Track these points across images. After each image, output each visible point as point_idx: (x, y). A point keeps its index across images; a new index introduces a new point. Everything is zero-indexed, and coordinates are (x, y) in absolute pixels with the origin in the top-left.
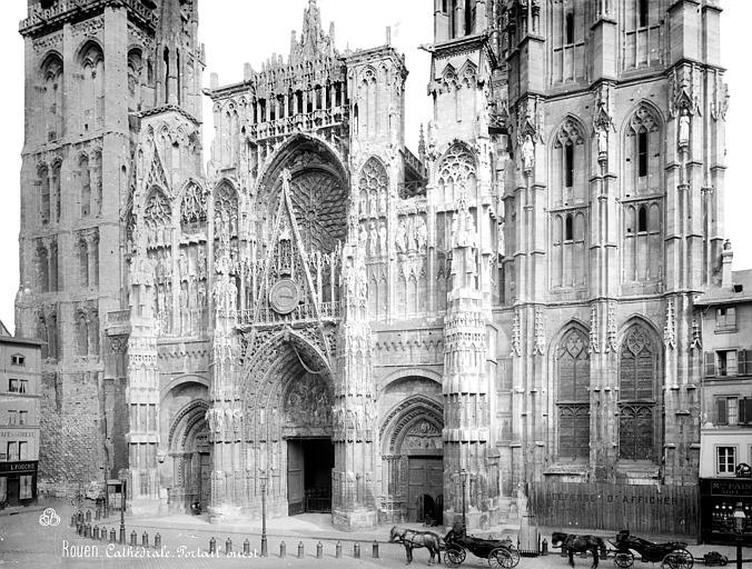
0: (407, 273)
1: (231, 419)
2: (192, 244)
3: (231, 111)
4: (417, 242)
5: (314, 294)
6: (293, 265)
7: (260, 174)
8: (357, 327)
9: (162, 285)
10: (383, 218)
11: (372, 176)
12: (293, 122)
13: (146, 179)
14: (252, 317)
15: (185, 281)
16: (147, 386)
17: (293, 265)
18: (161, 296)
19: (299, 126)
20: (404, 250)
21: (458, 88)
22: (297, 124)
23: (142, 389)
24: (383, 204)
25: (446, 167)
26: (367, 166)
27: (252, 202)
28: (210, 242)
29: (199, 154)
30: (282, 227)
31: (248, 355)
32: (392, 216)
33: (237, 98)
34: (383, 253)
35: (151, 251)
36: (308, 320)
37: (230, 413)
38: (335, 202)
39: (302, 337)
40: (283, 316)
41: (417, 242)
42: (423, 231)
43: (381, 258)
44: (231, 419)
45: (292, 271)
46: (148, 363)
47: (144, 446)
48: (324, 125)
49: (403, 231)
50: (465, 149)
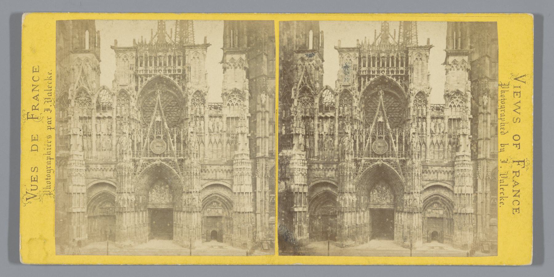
0: (213, 141)
1: (130, 200)
2: (104, 118)
3: (125, 59)
4: (218, 127)
5: (173, 147)
6: (162, 133)
7: (140, 89)
8: (193, 162)
9: (87, 134)
10: (202, 117)
11: (197, 98)
12: (157, 69)
13: (77, 83)
14: (140, 154)
15: (99, 135)
16: (81, 184)
17: (162, 133)
18: (85, 141)
19: (160, 71)
20: (212, 131)
21: (236, 68)
22: (159, 70)
23: (78, 185)
24: (202, 111)
25: (231, 99)
26: (195, 93)
27: (136, 101)
28: (114, 117)
29: (99, 75)
30: (157, 115)
31: (138, 171)
32: (206, 116)
33: (128, 53)
34: (203, 131)
35: (81, 118)
36: (169, 157)
37: (129, 197)
38: (173, 107)
39: (167, 165)
40: (157, 155)
41: (218, 127)
42: (220, 123)
43: (201, 133)
44: (130, 200)
45: (162, 136)
46: (81, 173)
47: (78, 214)
48: (172, 73)
49: (211, 123)
50: (239, 93)
